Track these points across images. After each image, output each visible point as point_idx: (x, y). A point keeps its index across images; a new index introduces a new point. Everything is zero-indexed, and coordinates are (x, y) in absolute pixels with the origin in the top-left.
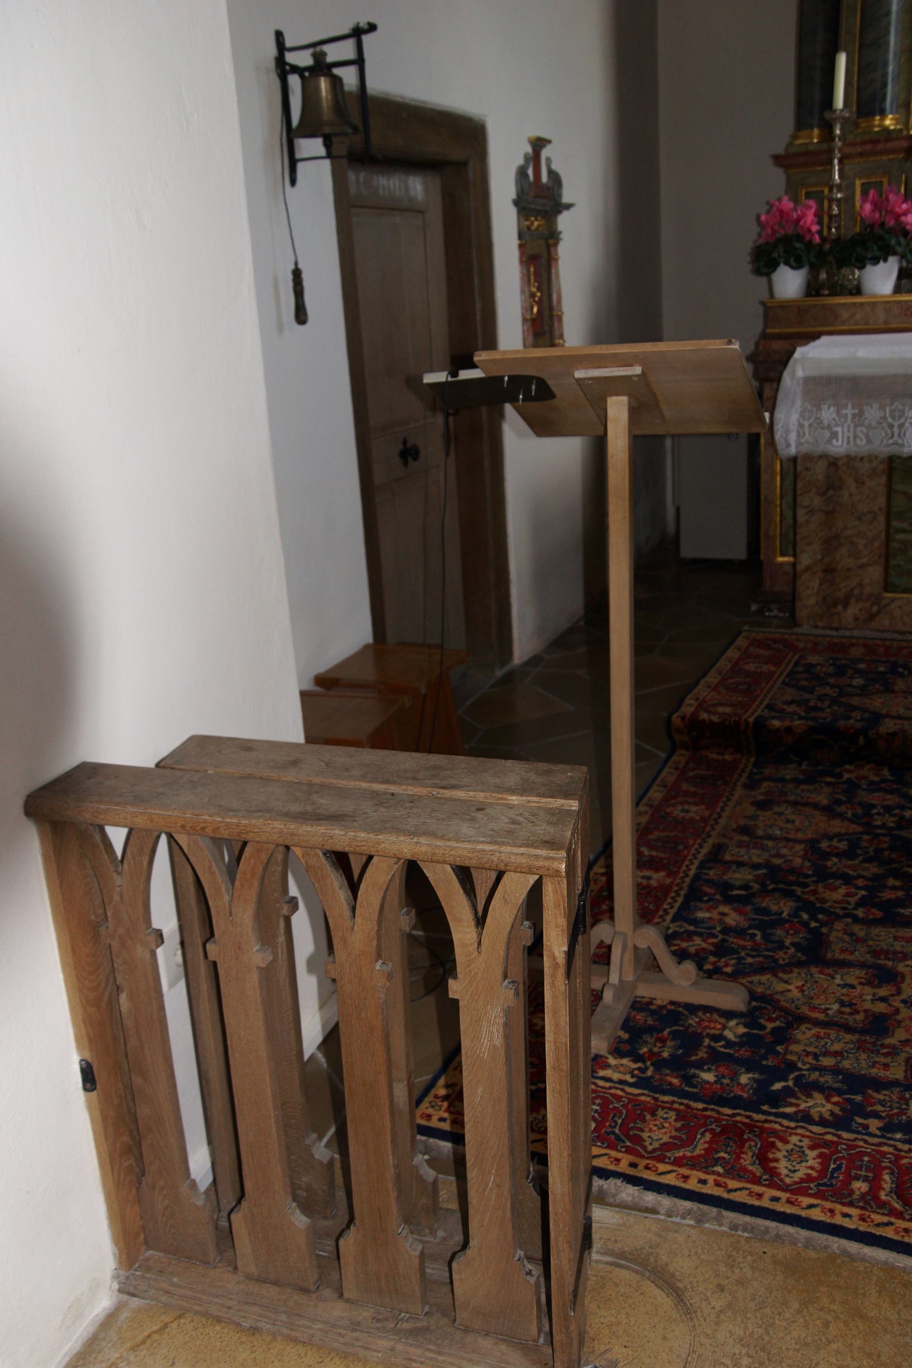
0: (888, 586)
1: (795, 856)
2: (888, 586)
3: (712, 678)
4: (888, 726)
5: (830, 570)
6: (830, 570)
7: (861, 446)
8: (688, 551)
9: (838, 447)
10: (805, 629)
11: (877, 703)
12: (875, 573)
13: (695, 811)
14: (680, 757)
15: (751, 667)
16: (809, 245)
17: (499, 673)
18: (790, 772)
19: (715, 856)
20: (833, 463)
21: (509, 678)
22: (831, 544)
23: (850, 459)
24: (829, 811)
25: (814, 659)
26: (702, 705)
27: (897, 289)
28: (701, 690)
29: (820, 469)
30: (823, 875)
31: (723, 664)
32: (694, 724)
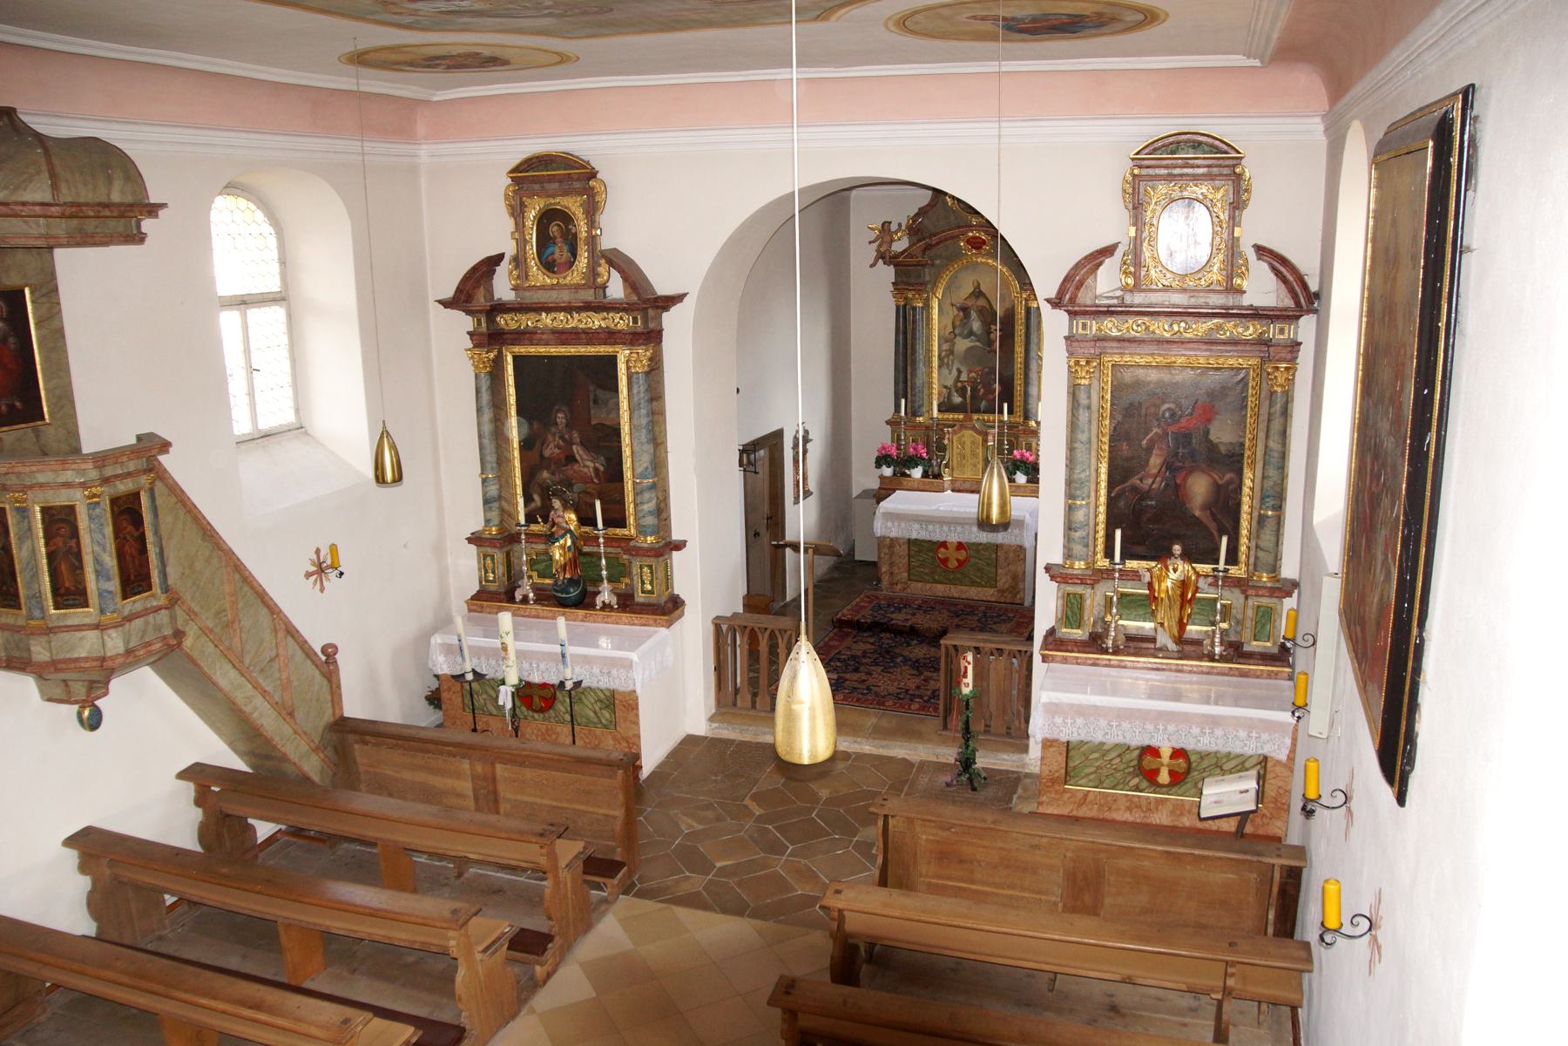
0: (909, 580)
1: (859, 653)
2: (909, 580)
3: (849, 607)
4: (894, 622)
5: (892, 573)
6: (892, 573)
7: (899, 535)
8: (857, 558)
9: (893, 535)
10: (884, 592)
11: (893, 616)
12: (905, 575)
13: (836, 643)
14: (836, 630)
15: (862, 604)
16: (893, 459)
17: (782, 604)
18: (866, 635)
19: (839, 653)
20: (892, 539)
21: (785, 606)
22: (891, 565)
23: (897, 539)
24: (872, 644)
25: (883, 602)
26: (843, 615)
27: (923, 477)
28: (845, 611)
29: (888, 541)
30: (864, 657)
31: (854, 603)
32: (840, 621)
